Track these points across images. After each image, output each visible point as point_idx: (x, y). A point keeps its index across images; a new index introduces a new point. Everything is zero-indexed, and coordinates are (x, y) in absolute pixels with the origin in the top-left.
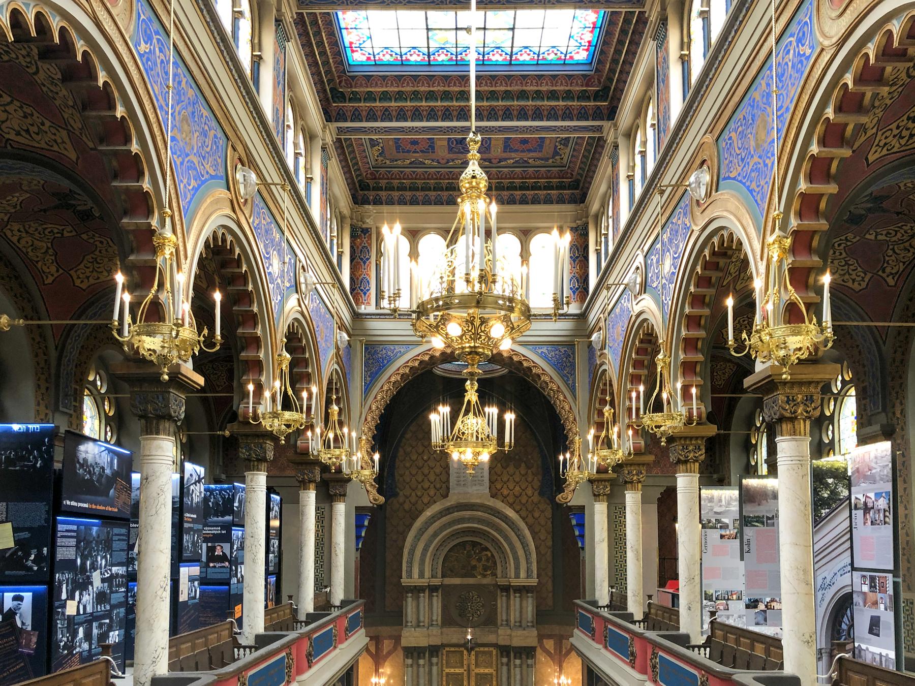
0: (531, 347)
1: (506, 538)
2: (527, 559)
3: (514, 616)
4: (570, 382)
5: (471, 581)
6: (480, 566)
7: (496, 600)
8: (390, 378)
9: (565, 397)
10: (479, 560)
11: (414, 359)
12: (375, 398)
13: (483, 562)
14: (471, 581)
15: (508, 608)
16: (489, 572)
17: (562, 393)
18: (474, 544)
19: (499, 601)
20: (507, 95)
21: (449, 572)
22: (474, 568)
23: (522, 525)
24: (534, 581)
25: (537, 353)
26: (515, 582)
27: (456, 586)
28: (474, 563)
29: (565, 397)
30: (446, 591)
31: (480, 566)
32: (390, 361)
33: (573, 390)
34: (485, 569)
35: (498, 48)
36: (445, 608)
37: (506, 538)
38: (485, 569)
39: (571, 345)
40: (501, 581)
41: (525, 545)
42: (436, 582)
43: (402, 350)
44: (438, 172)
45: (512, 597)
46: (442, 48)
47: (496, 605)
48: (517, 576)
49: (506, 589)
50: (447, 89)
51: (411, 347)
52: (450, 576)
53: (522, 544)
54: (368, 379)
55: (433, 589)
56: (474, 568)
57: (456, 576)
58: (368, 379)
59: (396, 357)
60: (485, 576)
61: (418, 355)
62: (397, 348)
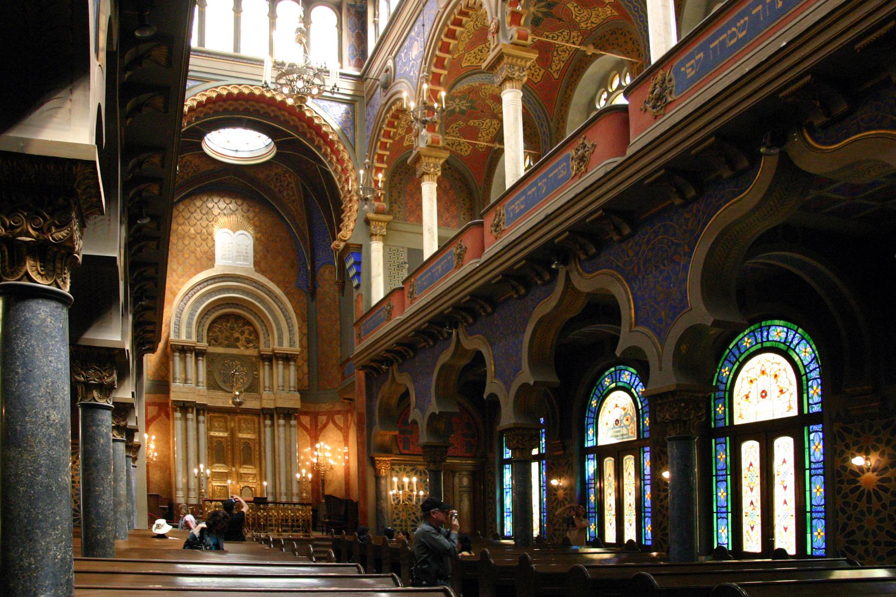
1: (271, 311)
2: (290, 331)
3: (279, 379)
5: (234, 351)
6: (242, 338)
7: (257, 370)
10: (243, 333)
13: (246, 335)
14: (234, 351)
15: (271, 375)
16: (251, 345)
18: (238, 318)
19: (261, 371)
21: (213, 342)
22: (237, 339)
23: (285, 299)
24: (296, 349)
26: (279, 349)
27: (219, 354)
28: (236, 335)
30: (211, 359)
31: (242, 338)
34: (248, 341)
36: (209, 373)
37: (271, 311)
38: (248, 341)
40: (265, 350)
41: (287, 318)
42: (203, 345)
45: (274, 366)
47: (258, 375)
48: (281, 343)
49: (271, 359)
52: (213, 345)
53: (285, 316)
55: (199, 354)
56: (237, 339)
57: (220, 345)
60: (248, 348)
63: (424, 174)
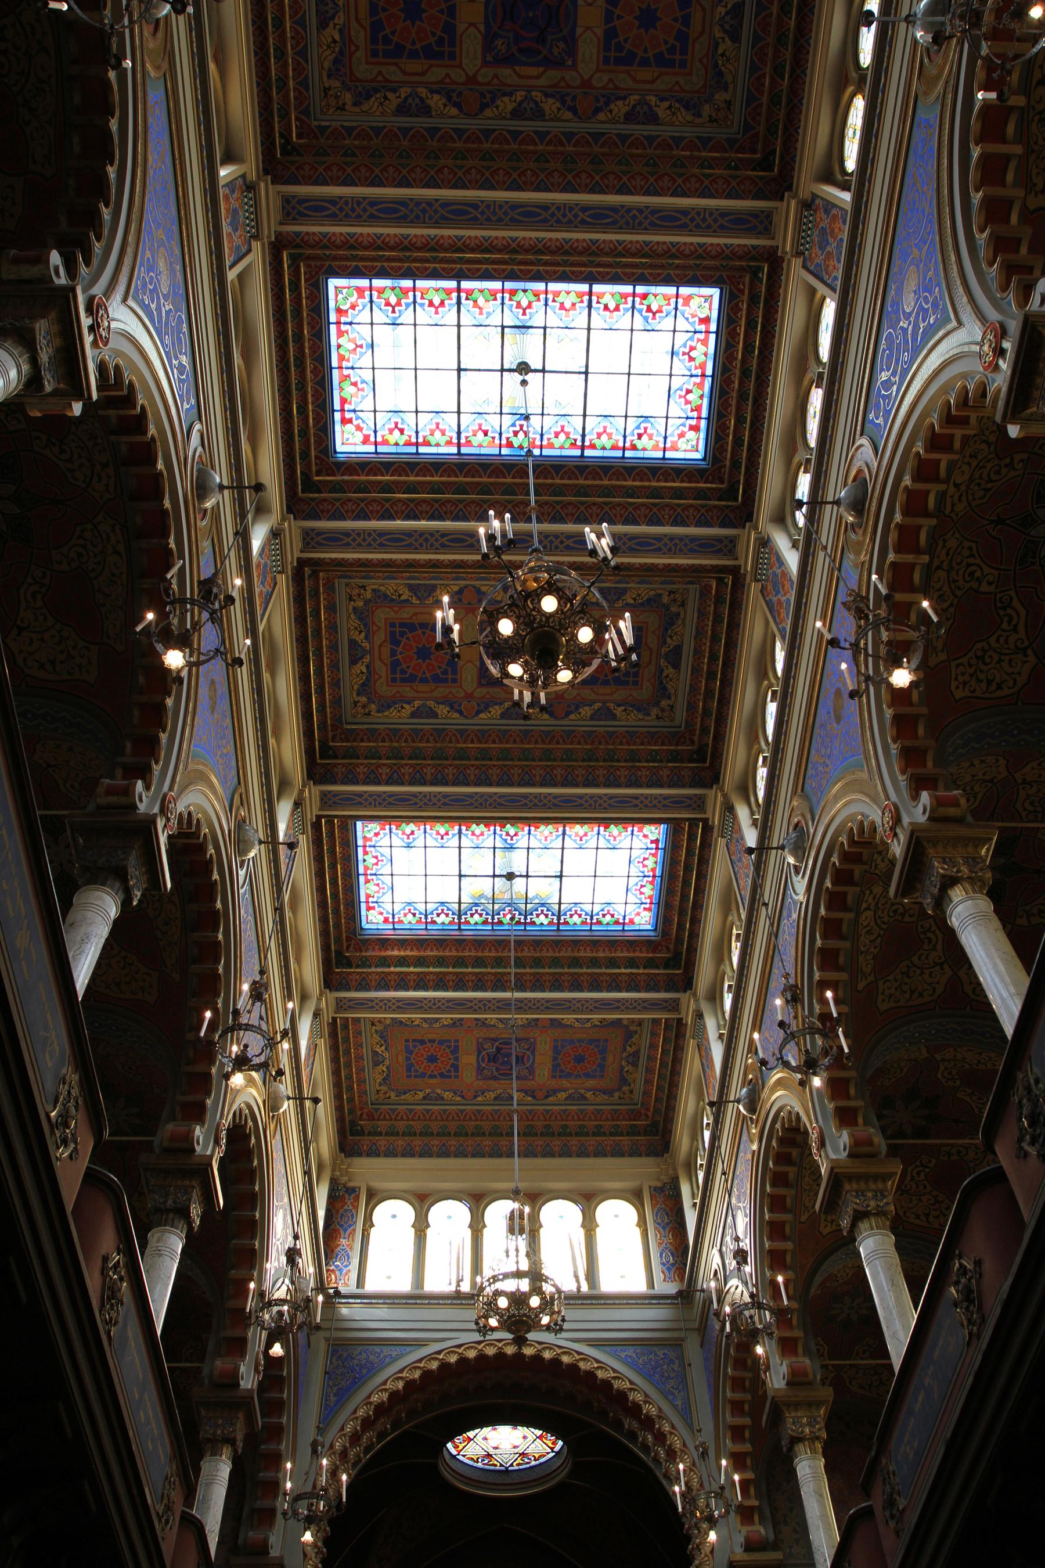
0: (608, 1349)
4: (679, 1403)
8: (369, 1397)
9: (673, 1427)
11: (412, 1367)
12: (342, 1429)
17: (668, 1420)
20: (556, 962)
25: (619, 1358)
29: (673, 1427)
32: (372, 1369)
33: (686, 1414)
35: (543, 905)
39: (676, 1344)
43: (394, 1354)
44: (462, 1111)
46: (476, 905)
50: (480, 954)
51: (408, 1349)
54: (333, 1399)
58: (333, 1399)
59: (383, 1366)
61: (420, 1360)
62: (386, 1351)
63: (795, 1440)
